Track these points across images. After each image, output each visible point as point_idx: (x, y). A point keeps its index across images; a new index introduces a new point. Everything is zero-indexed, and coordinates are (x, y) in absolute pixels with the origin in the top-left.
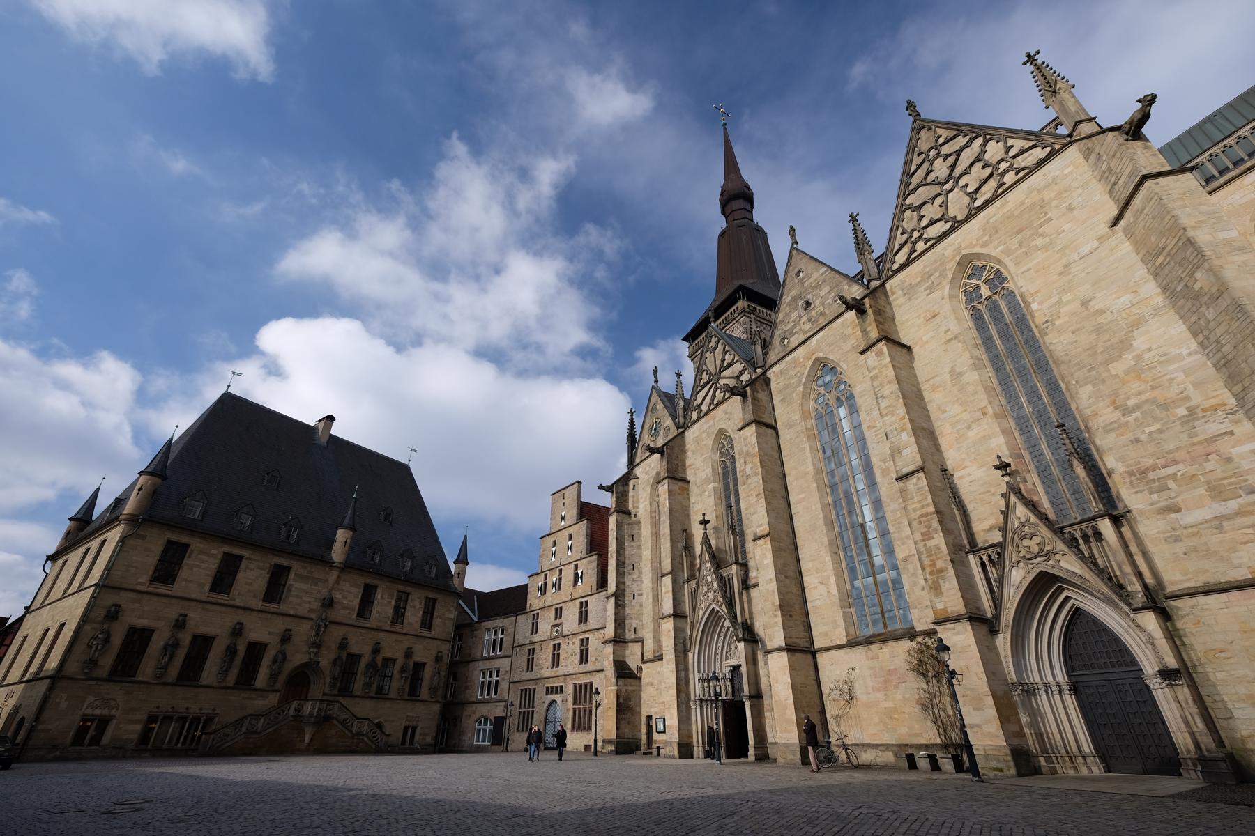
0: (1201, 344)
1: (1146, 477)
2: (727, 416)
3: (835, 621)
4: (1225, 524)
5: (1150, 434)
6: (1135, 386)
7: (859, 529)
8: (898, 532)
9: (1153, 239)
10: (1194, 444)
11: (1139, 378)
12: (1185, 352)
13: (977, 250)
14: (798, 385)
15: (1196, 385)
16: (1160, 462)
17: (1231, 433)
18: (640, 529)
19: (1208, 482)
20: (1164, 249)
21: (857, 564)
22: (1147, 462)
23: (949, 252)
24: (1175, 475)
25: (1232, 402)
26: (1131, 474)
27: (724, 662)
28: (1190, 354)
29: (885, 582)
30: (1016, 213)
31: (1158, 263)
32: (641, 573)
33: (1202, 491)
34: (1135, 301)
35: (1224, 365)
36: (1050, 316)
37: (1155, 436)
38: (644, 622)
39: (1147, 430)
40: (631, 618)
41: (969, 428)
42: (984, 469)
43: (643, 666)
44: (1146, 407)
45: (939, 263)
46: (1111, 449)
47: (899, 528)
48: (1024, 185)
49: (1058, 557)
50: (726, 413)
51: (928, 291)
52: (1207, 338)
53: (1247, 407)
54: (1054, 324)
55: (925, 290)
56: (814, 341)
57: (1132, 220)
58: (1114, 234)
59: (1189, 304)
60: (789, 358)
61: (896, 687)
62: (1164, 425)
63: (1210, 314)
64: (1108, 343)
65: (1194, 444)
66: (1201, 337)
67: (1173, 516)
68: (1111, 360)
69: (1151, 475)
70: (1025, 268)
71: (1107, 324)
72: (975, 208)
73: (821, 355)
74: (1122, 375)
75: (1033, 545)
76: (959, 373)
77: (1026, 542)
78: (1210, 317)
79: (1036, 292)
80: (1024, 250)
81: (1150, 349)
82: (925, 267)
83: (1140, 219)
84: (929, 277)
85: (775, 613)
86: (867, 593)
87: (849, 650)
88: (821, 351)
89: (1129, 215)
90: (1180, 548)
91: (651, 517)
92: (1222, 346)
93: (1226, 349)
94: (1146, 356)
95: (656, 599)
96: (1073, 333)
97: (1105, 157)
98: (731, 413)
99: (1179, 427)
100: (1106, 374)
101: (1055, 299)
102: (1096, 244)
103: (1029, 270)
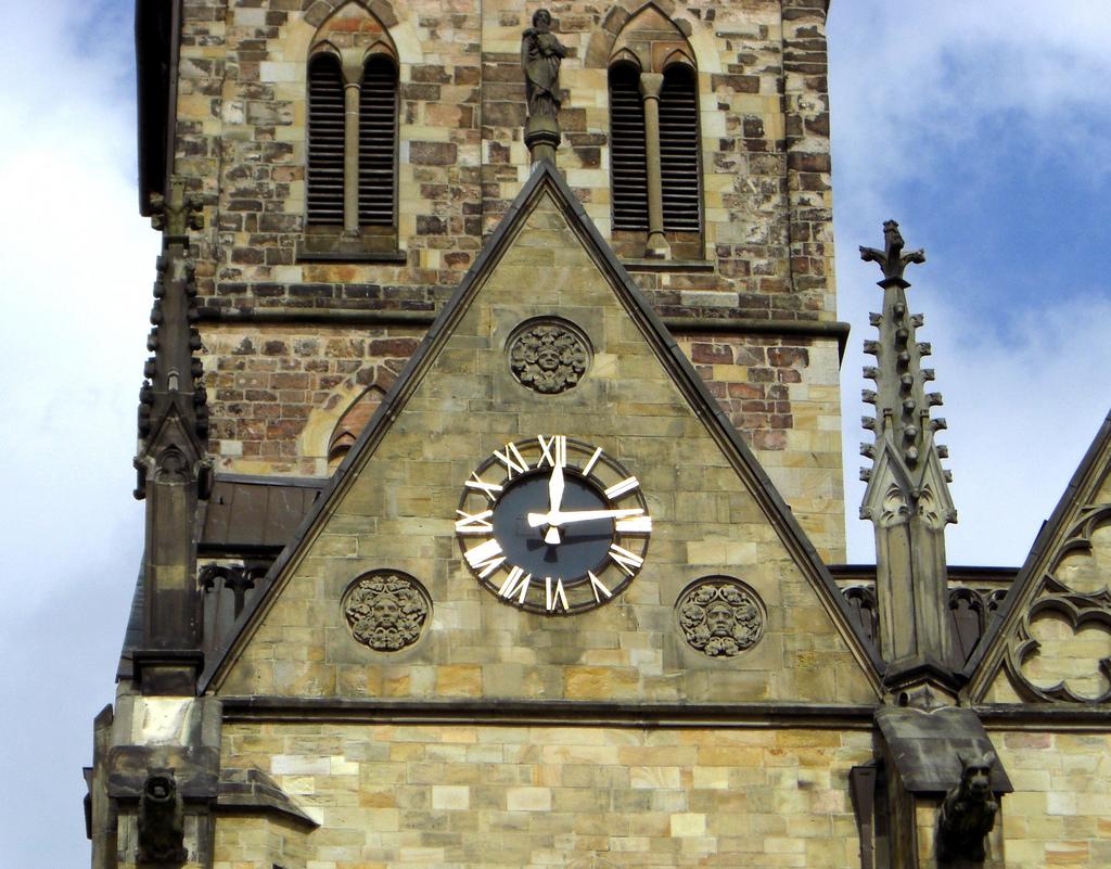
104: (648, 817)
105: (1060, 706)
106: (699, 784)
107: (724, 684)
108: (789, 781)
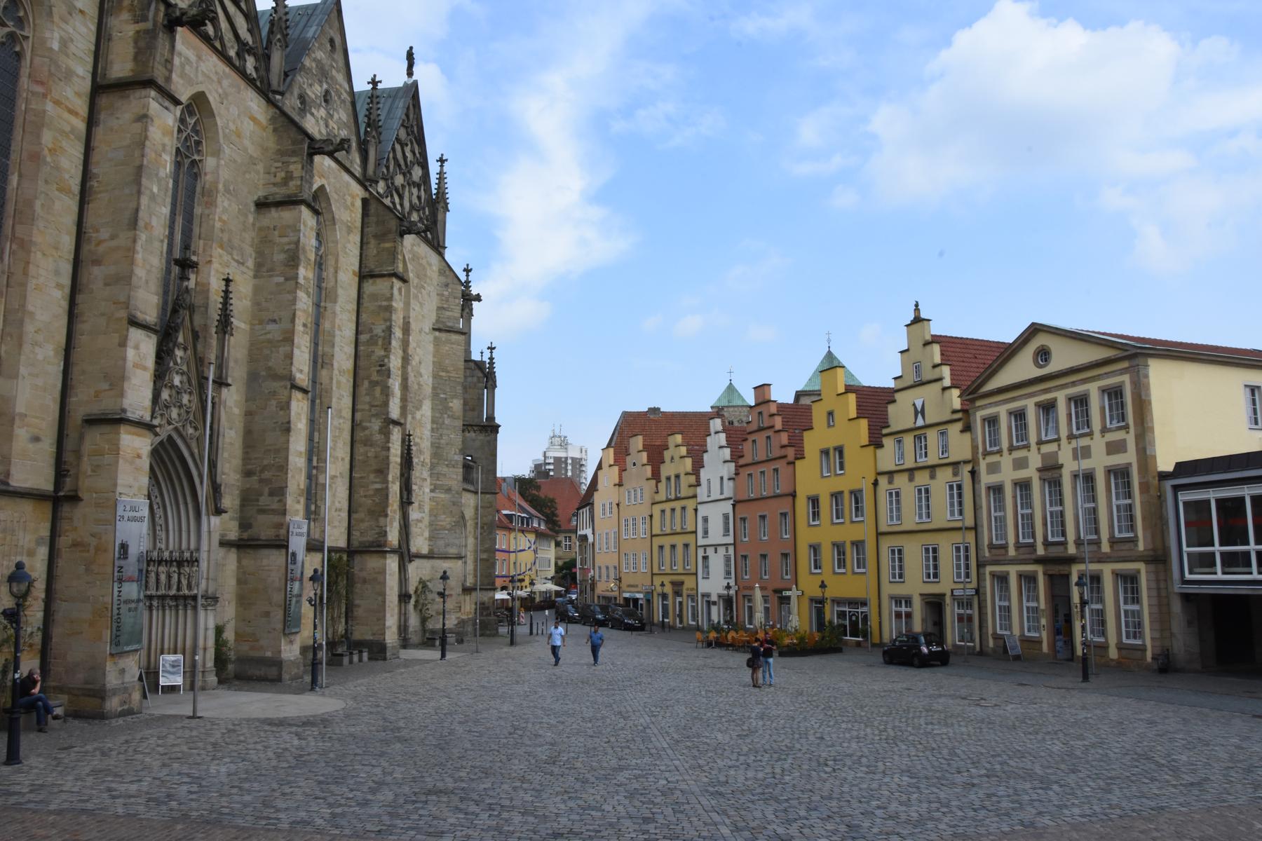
35: (437, 447)
52: (437, 429)
59: (440, 407)
63: (447, 421)
66: (435, 426)
78: (446, 422)
85: (299, 498)
89: (443, 336)
93: (442, 441)
97: (450, 290)
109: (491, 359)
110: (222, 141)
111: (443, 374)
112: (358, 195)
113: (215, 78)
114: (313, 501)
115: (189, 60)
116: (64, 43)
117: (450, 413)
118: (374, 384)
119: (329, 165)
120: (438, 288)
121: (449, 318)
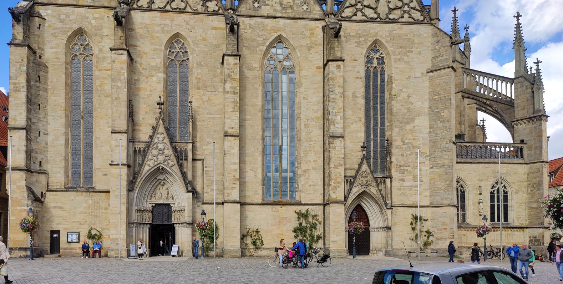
0: (430, 132)
1: (401, 168)
2: (188, 27)
3: (256, 191)
4: (412, 188)
5: (407, 154)
6: (410, 136)
7: (278, 148)
8: (305, 157)
9: (439, 89)
10: (415, 162)
11: (412, 133)
12: (425, 132)
13: (383, 41)
14: (263, 44)
15: (423, 144)
16: (406, 164)
17: (424, 162)
18: (47, 72)
19: (414, 175)
20: (440, 95)
21: (272, 164)
22: (403, 163)
23: (372, 31)
24: (407, 170)
25: (428, 153)
26: (397, 165)
27: (148, 201)
28: (426, 133)
29: (285, 178)
30: (404, 37)
31: (434, 97)
32: (47, 115)
33: (411, 177)
34: (421, 106)
35: (433, 142)
36: (397, 94)
37: (408, 156)
38: (49, 158)
39: (407, 152)
40: (37, 152)
41: (352, 123)
42: (352, 144)
43: (48, 194)
44: (409, 145)
45: (366, 33)
46: (395, 154)
47: (306, 155)
48: (411, 27)
49: (371, 187)
50: (187, 24)
51: (356, 45)
53: (431, 157)
54: (397, 98)
55: (356, 43)
56: (282, 22)
57: (436, 76)
58: (426, 76)
59: (435, 118)
60: (259, 20)
61: (285, 225)
62: (411, 153)
64: (409, 116)
65: (415, 162)
67: (402, 182)
68: (407, 123)
69: (402, 168)
70: (397, 66)
71: (411, 109)
72: (391, 19)
73: (284, 35)
74: (408, 130)
75: (364, 180)
76: (356, 96)
77: (362, 179)
79: (396, 80)
80: (399, 57)
81: (418, 126)
82: (359, 30)
83: (438, 79)
84: (360, 37)
86: (274, 180)
87: (262, 206)
88: (285, 33)
89: (435, 73)
90: (400, 192)
91: (66, 68)
92: (437, 136)
94: (416, 127)
95: (67, 142)
96: (401, 106)
97: (440, 44)
98: (193, 27)
99: (414, 155)
100: (404, 127)
101: (401, 88)
102: (420, 75)
103: (398, 68)
104: (88, 20)
105: (141, 8)
106: (94, 16)
107: (99, 3)
108: (106, 16)
109: (538, 70)
110: (192, 47)
111: (437, 97)
112: (317, 27)
113: (185, 23)
114: (296, 183)
115: (166, 24)
116: (100, 50)
117: (442, 120)
118: (327, 119)
119: (284, 24)
120: (432, 46)
121: (440, 61)
